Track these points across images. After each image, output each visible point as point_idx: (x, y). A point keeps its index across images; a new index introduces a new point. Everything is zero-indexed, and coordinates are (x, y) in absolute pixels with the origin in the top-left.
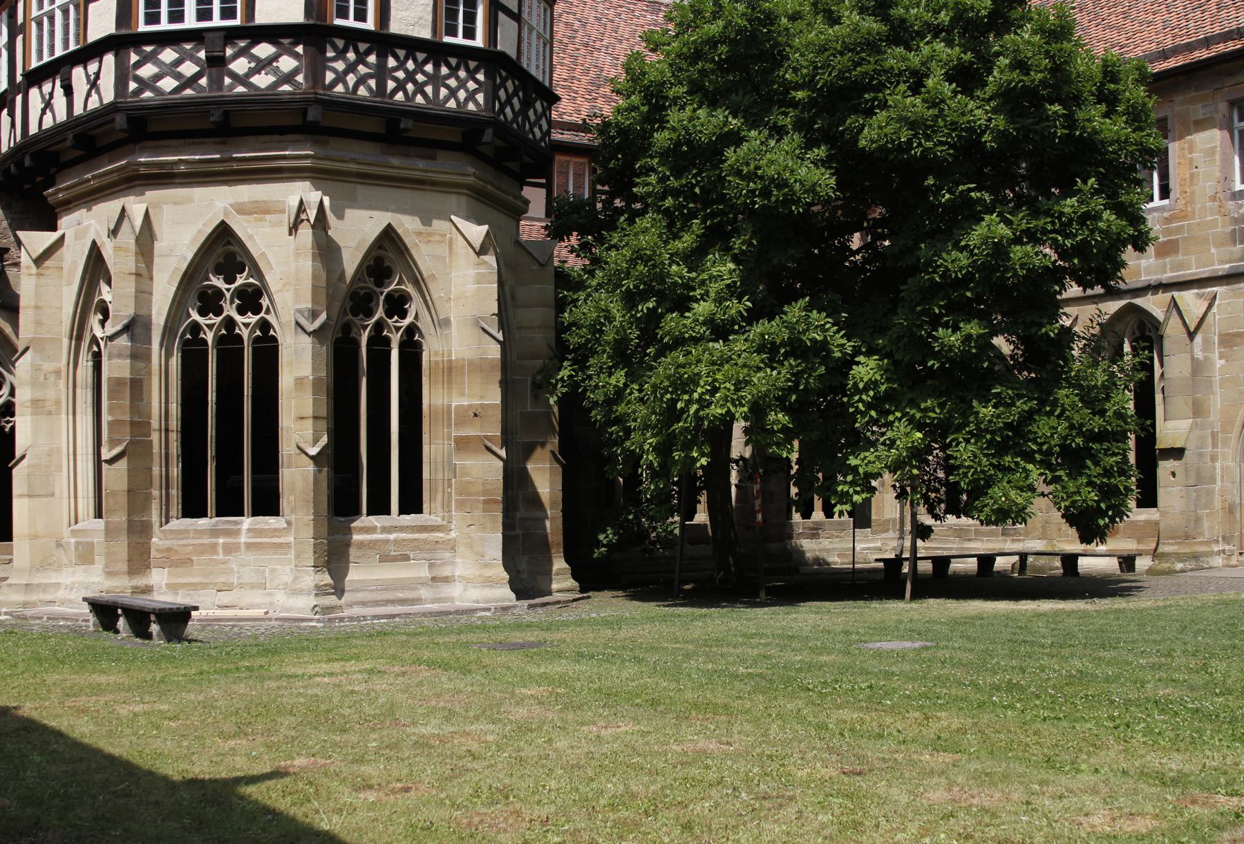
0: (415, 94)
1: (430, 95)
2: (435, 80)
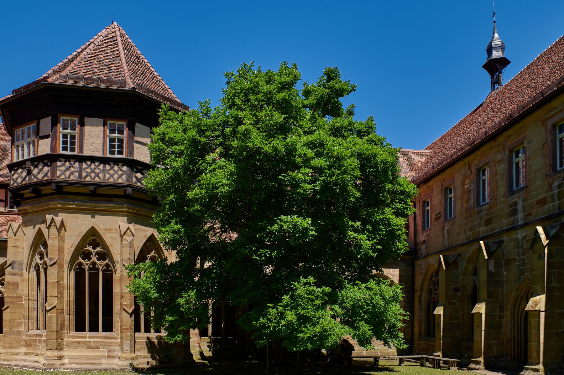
0: (95, 177)
1: (102, 177)
2: (104, 171)
